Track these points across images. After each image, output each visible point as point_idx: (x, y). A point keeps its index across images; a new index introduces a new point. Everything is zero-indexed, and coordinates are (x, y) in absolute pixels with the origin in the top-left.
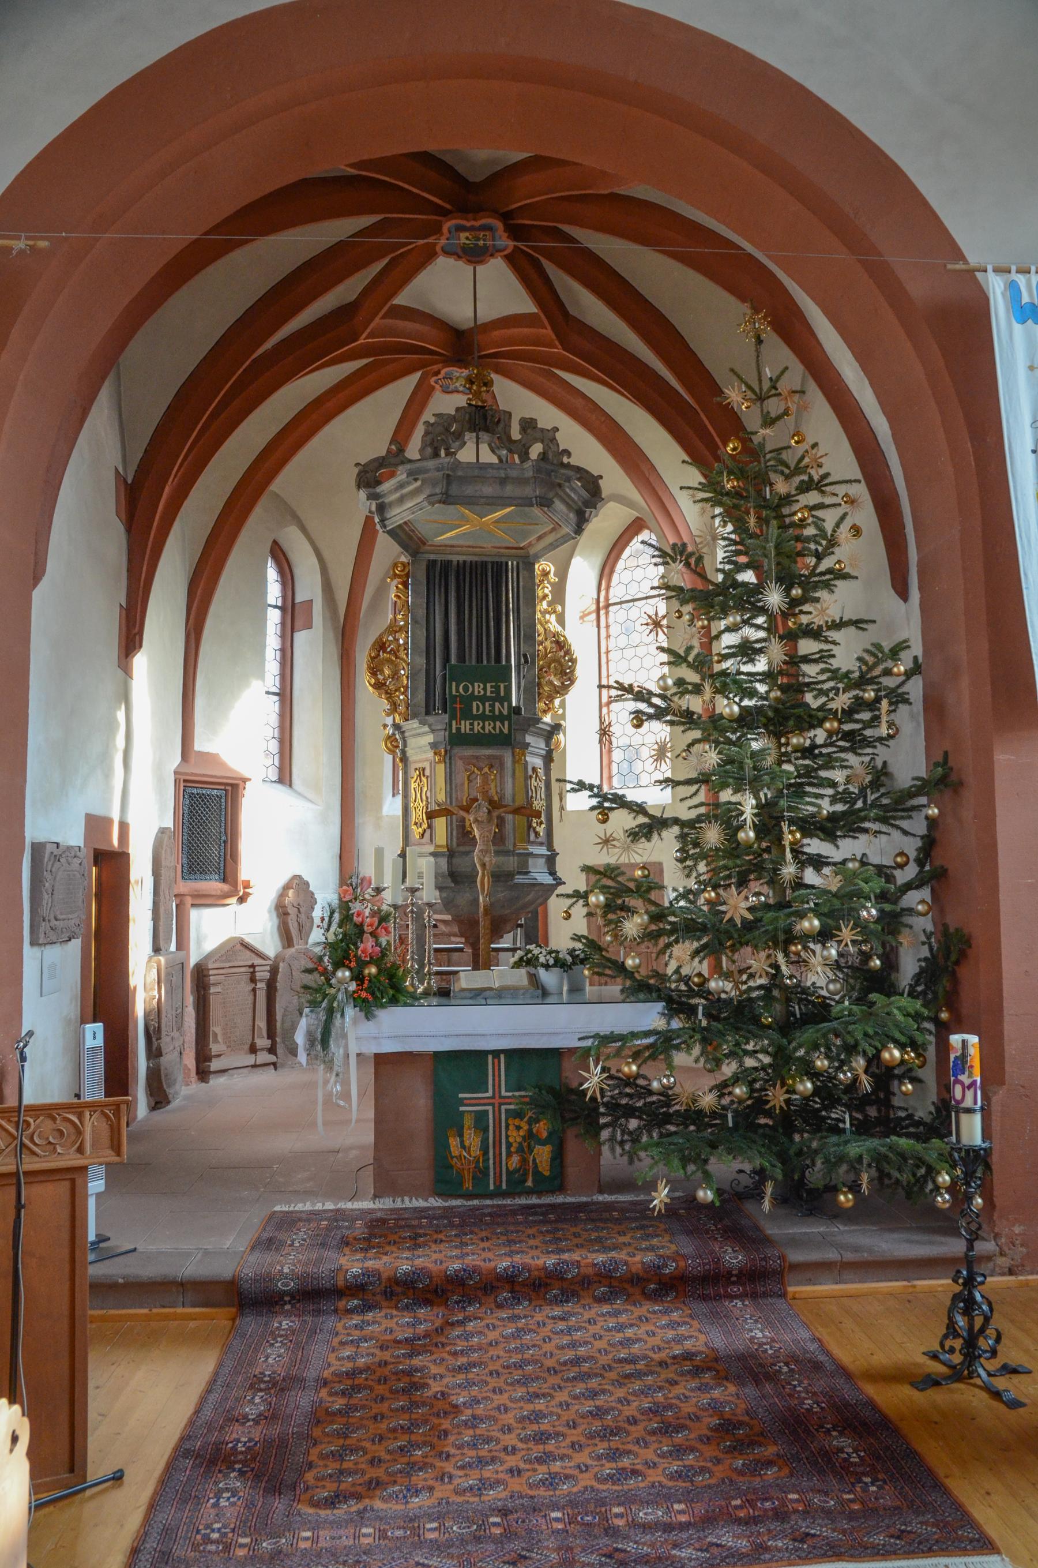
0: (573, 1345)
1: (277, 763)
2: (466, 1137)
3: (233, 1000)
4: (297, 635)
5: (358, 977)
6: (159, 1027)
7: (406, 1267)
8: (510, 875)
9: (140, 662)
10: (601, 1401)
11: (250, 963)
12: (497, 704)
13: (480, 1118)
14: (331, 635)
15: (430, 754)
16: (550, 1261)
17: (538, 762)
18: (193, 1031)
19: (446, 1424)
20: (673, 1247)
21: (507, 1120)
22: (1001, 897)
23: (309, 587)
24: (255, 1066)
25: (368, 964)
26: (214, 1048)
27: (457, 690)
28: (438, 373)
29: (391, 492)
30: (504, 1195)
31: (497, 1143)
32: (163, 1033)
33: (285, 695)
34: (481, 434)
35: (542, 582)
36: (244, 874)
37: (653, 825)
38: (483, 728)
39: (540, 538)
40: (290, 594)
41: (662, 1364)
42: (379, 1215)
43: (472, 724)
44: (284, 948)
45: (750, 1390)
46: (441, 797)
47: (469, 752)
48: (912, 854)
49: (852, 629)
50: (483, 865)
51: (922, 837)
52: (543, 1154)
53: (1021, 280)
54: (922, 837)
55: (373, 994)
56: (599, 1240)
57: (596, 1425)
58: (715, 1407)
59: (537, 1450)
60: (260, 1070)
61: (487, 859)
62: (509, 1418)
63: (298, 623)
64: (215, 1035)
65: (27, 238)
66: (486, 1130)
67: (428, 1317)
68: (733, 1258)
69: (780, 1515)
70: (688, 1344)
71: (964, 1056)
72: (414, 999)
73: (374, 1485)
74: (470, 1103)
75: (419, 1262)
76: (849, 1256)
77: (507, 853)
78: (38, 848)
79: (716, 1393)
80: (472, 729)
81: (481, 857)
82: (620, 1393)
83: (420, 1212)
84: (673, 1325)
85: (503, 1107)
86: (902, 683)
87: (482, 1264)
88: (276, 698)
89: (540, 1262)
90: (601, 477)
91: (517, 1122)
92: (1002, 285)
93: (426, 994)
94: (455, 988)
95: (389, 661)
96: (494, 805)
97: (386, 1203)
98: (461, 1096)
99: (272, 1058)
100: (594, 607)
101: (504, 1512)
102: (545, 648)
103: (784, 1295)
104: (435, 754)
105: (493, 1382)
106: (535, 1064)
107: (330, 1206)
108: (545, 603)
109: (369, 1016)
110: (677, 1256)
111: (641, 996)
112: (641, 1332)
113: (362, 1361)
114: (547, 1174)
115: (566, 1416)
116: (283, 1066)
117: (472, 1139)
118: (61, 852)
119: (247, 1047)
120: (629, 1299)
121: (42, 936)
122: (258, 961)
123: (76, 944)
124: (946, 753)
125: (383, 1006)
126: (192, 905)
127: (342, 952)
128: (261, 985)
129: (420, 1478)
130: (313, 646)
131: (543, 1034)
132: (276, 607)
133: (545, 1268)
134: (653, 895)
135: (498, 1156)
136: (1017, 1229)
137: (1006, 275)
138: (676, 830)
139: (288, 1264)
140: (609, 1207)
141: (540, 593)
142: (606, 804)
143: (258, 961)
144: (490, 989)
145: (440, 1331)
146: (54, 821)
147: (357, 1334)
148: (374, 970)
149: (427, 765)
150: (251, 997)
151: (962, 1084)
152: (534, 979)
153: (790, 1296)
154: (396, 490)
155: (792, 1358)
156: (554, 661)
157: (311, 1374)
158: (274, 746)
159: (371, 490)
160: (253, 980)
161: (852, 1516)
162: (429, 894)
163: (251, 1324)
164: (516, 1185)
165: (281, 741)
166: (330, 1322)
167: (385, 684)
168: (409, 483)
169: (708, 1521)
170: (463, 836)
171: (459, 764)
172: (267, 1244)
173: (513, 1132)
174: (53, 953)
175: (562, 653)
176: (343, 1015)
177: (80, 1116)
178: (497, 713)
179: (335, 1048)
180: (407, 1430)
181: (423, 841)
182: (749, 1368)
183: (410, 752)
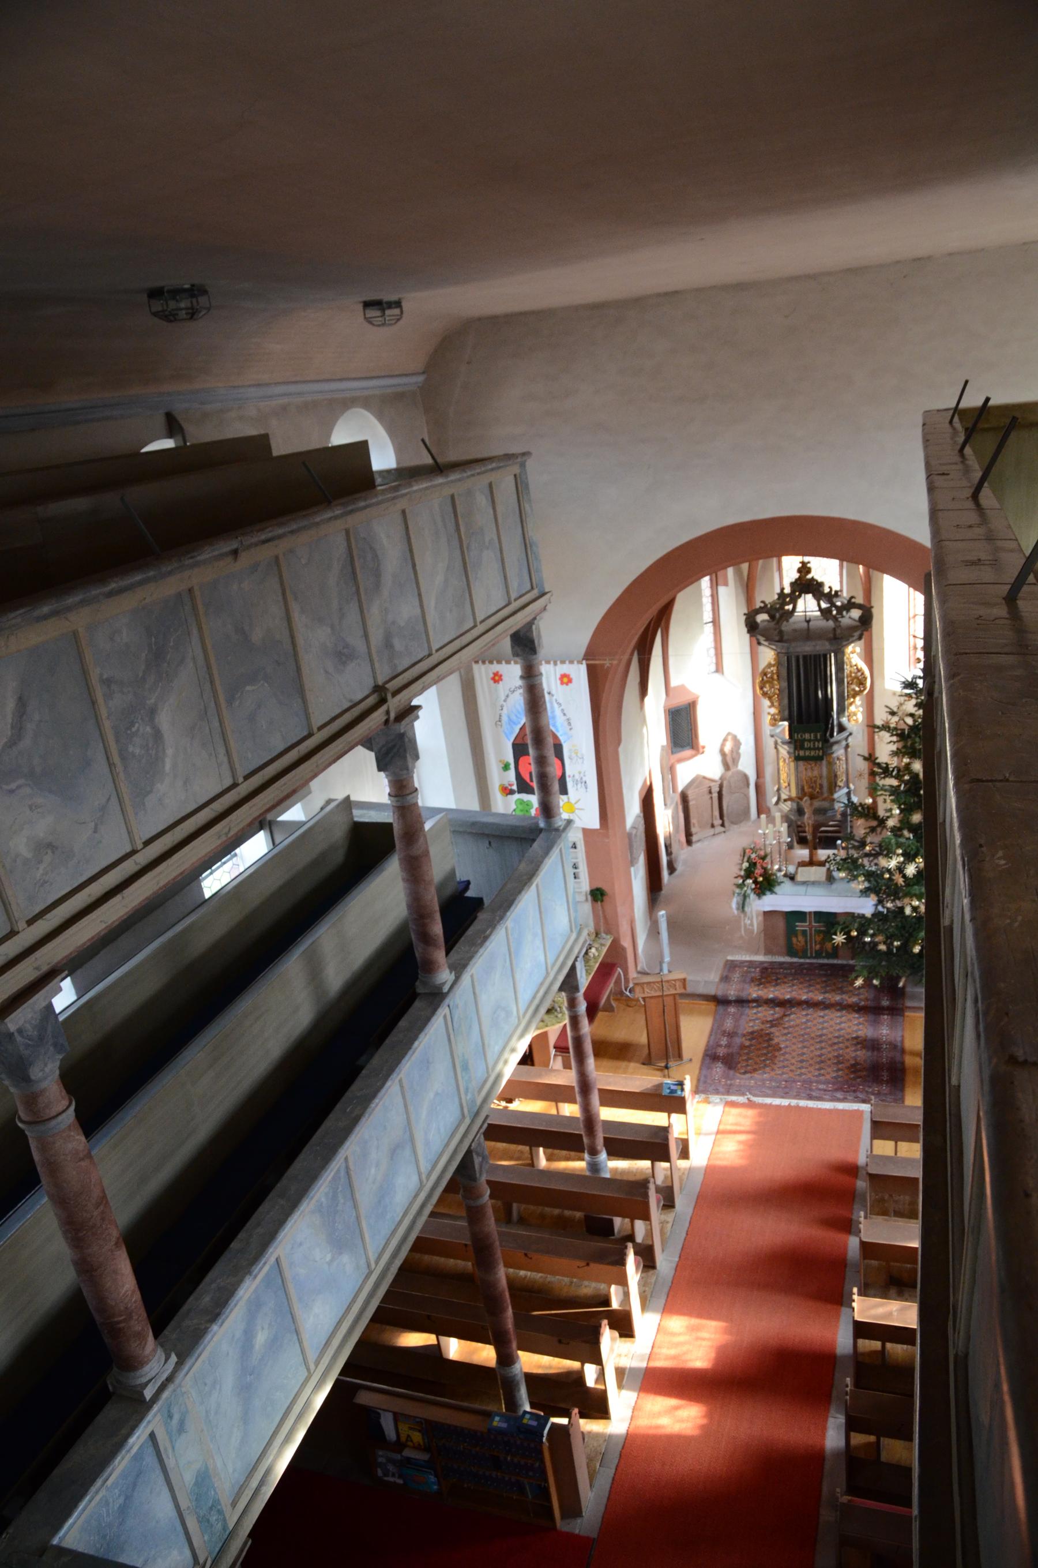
3: (701, 805)
5: (755, 882)
7: (771, 996)
10: (824, 1051)
13: (804, 932)
14: (740, 590)
16: (820, 998)
26: (693, 830)
30: (815, 958)
33: (716, 622)
41: (848, 1040)
45: (869, 1054)
56: (841, 989)
58: (855, 1058)
59: (800, 1065)
63: (720, 581)
69: (854, 1091)
73: (755, 1070)
74: (801, 926)
75: (777, 993)
83: (781, 964)
99: (722, 829)
105: (794, 1040)
107: (748, 958)
110: (867, 999)
117: (800, 938)
122: (712, 784)
129: (768, 1069)
135: (811, 947)
139: (732, 993)
145: (782, 1018)
147: (755, 1017)
155: (890, 1043)
157: (740, 1032)
158: (712, 652)
160: (710, 792)
163: (721, 1008)
164: (818, 955)
166: (747, 1011)
169: (836, 1090)
170: (800, 812)
172: (725, 979)
182: (873, 1045)
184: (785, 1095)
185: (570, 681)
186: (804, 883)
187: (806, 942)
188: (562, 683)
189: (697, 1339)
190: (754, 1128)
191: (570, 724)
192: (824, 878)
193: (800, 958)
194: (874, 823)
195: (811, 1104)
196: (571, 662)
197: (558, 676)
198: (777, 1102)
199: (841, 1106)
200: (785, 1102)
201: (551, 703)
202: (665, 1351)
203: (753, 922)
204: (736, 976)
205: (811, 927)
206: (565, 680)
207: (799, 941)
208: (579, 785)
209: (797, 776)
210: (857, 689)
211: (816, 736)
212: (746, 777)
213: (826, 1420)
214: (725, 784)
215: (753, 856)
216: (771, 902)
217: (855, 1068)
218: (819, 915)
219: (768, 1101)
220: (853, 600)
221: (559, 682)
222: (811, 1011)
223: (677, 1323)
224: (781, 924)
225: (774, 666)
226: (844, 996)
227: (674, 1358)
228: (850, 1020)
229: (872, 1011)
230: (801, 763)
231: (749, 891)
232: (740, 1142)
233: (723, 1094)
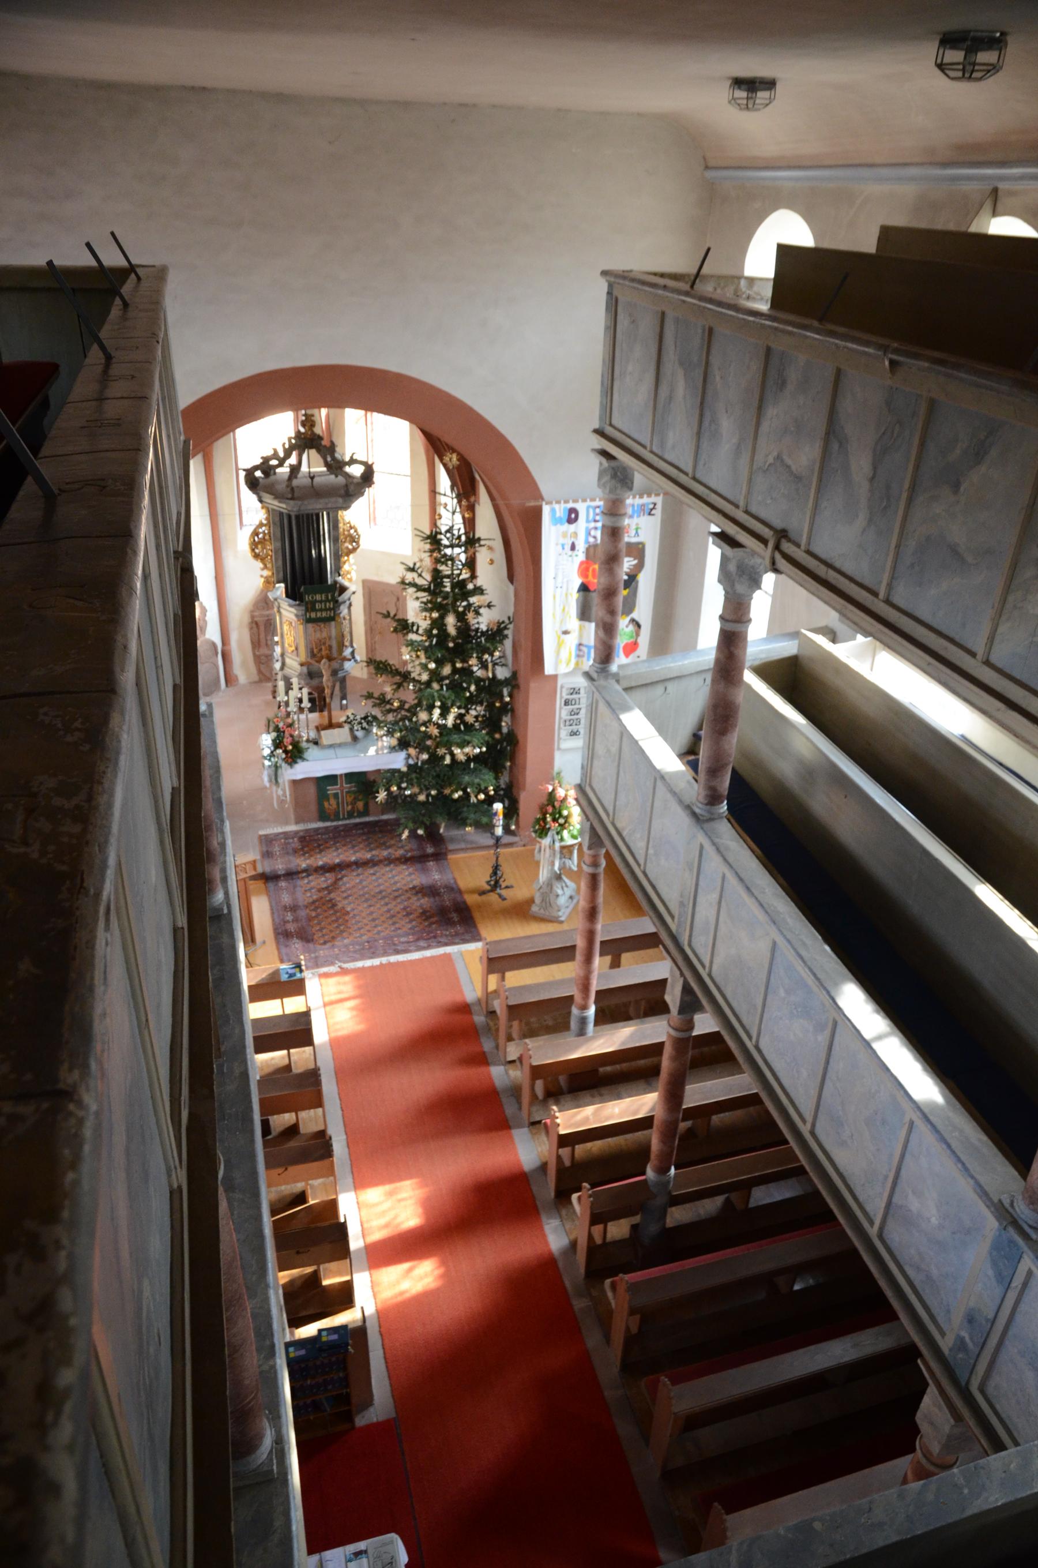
0: (379, 885)
5: (286, 752)
10: (389, 906)
13: (336, 796)
16: (369, 856)
41: (407, 891)
42: (302, 834)
45: (432, 900)
52: (360, 805)
53: (556, 506)
56: (384, 844)
58: (421, 906)
59: (373, 924)
67: (330, 877)
68: (430, 850)
69: (435, 937)
73: (333, 938)
74: (332, 790)
76: (469, 846)
79: (422, 901)
82: (394, 903)
83: (316, 830)
84: (410, 874)
110: (411, 850)
113: (315, 897)
117: (333, 802)
139: (280, 866)
155: (446, 887)
157: (301, 904)
161: (452, 936)
163: (271, 885)
164: (350, 815)
166: (299, 882)
169: (418, 940)
172: (267, 855)
179: (280, 780)
180: (336, 921)
182: (431, 891)
184: (374, 955)
186: (331, 746)
187: (338, 804)
189: (400, 1201)
192: (349, 739)
193: (332, 821)
194: (398, 679)
198: (368, 963)
199: (428, 953)
200: (376, 962)
202: (376, 1223)
203: (284, 792)
204: (276, 849)
205: (342, 788)
207: (331, 805)
209: (306, 639)
210: (350, 547)
212: (214, 645)
213: (542, 1229)
215: (281, 725)
216: (302, 770)
217: (425, 915)
218: (350, 777)
219: (359, 964)
222: (360, 870)
223: (374, 1194)
225: (265, 525)
226: (390, 850)
227: (386, 1226)
228: (400, 873)
229: (419, 859)
230: (310, 625)
231: (280, 762)
232: (352, 1009)
233: (313, 968)
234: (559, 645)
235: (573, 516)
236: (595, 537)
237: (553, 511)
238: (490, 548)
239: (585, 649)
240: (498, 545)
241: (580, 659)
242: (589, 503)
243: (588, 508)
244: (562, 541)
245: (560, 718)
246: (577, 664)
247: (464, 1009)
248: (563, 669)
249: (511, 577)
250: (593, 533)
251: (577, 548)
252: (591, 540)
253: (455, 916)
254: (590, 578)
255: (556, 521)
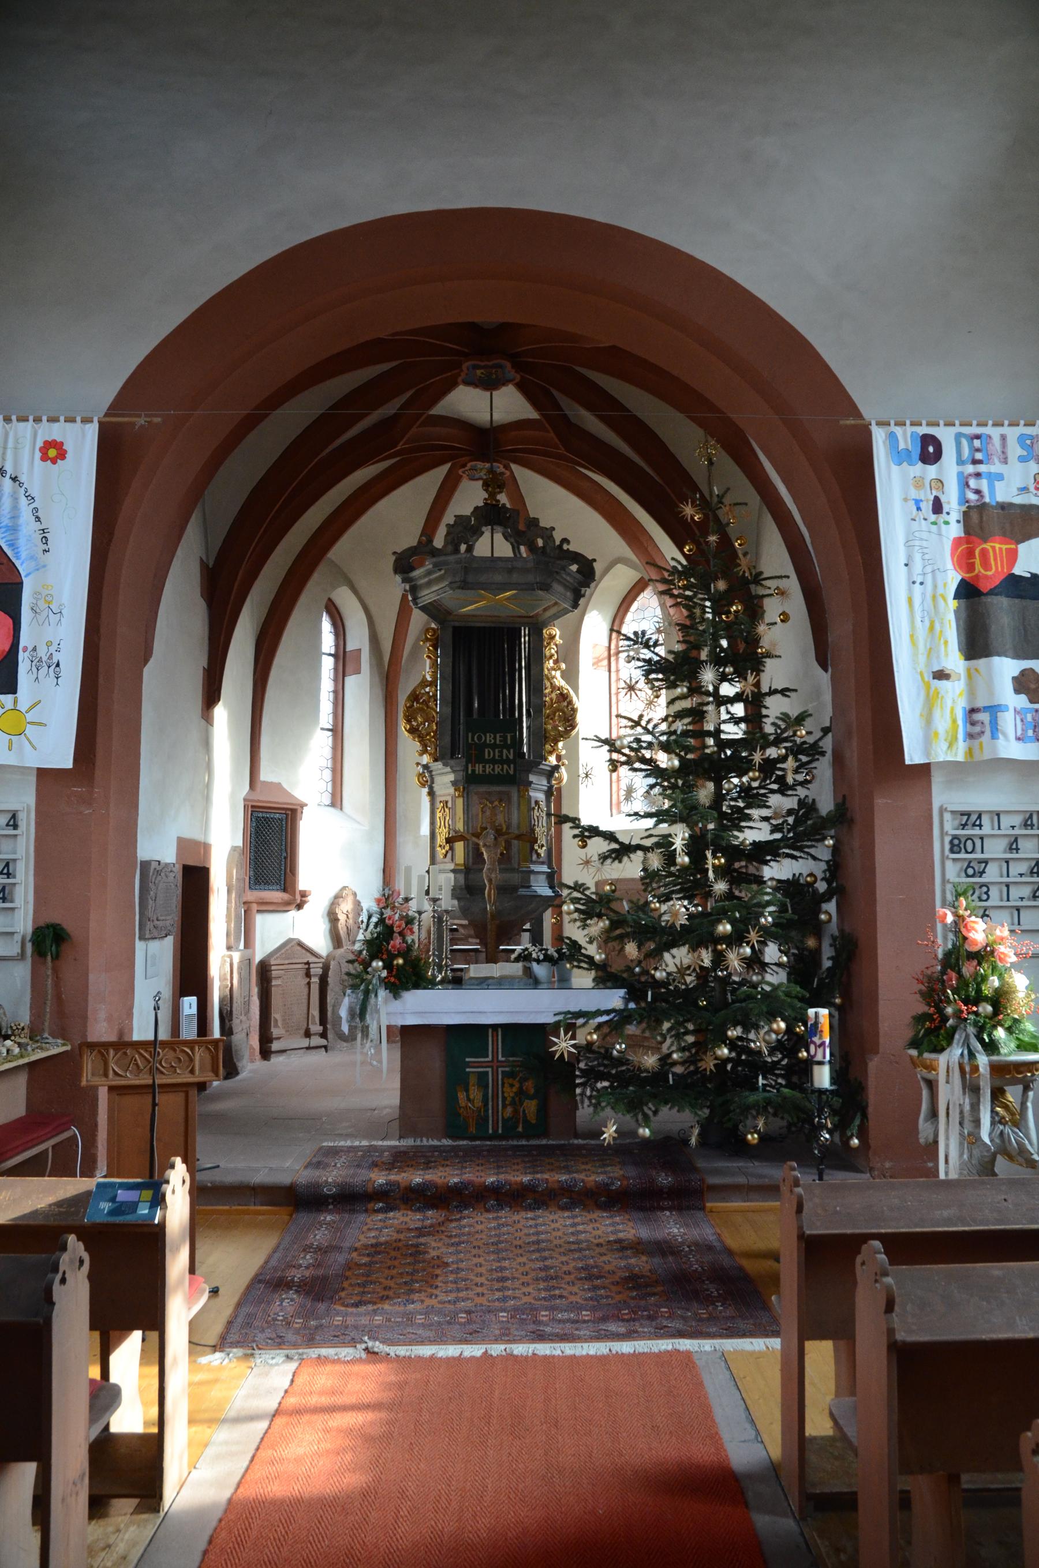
1: (330, 789)
2: (471, 1092)
3: (291, 993)
4: (347, 679)
6: (231, 1011)
7: (418, 1180)
8: (515, 889)
9: (220, 712)
11: (305, 961)
12: (505, 751)
14: (377, 679)
15: (452, 790)
17: (541, 796)
18: (258, 1017)
19: (438, 1272)
20: (621, 1172)
21: (502, 1079)
22: (878, 909)
23: (358, 639)
24: (308, 1048)
25: (396, 957)
26: (275, 1032)
27: (473, 739)
28: (464, 466)
29: (420, 578)
30: (501, 1138)
31: (495, 1096)
32: (234, 1016)
33: (337, 731)
34: (495, 527)
35: (549, 644)
36: (302, 885)
37: (623, 851)
38: (493, 770)
39: (545, 610)
40: (342, 643)
41: (599, 1245)
42: (402, 1149)
43: (484, 767)
44: (334, 948)
46: (460, 826)
47: (483, 789)
48: (820, 875)
49: (779, 696)
50: (490, 881)
51: (827, 862)
52: (531, 1106)
53: (898, 431)
54: (827, 862)
55: (400, 980)
56: (566, 1167)
57: (543, 1274)
58: (627, 1268)
60: (314, 1052)
61: (493, 876)
62: (483, 1270)
63: (348, 669)
64: (276, 1021)
65: (146, 416)
66: (487, 1086)
68: (664, 1179)
70: (621, 1235)
71: (816, 1023)
72: (431, 984)
73: (384, 1298)
75: (428, 1177)
76: (754, 1181)
77: (513, 870)
78: (145, 865)
79: (633, 1261)
80: (484, 771)
81: (489, 875)
83: (434, 1148)
85: (500, 1070)
86: (820, 739)
87: (475, 1179)
88: (330, 733)
89: (519, 1179)
90: (595, 560)
91: (511, 1081)
92: (883, 435)
93: (442, 982)
94: (466, 977)
95: (421, 710)
96: (499, 832)
97: (409, 1142)
98: (467, 1060)
99: (323, 1042)
100: (606, 654)
101: (469, 1312)
102: (551, 699)
103: (703, 1209)
104: (456, 790)
106: (527, 1039)
107: (365, 1143)
108: (551, 661)
109: (396, 996)
111: (609, 984)
112: (589, 1228)
113: (383, 1239)
114: (534, 1122)
115: (521, 1269)
116: (333, 1049)
117: (475, 1093)
118: (161, 868)
119: (302, 1032)
120: (586, 1208)
121: (148, 932)
122: (312, 959)
123: (170, 940)
124: (844, 796)
125: (407, 989)
126: (258, 911)
127: (377, 946)
128: (315, 980)
129: (416, 1296)
130: (360, 689)
131: (531, 1012)
132: (330, 655)
133: (522, 1183)
134: (614, 905)
136: (888, 1165)
137: (888, 428)
138: (640, 853)
139: (333, 1176)
140: (580, 1147)
141: (548, 653)
142: (586, 834)
143: (312, 959)
144: (493, 978)
146: (158, 846)
147: (380, 1225)
148: (401, 961)
149: (449, 799)
150: (306, 990)
151: (815, 1043)
152: (528, 972)
153: (707, 1209)
154: (425, 576)
156: (559, 710)
158: (328, 775)
159: (406, 575)
160: (308, 975)
162: (447, 902)
163: (304, 1218)
165: (334, 770)
166: (362, 1217)
167: (417, 730)
168: (434, 572)
169: (604, 1319)
170: (475, 856)
171: (475, 799)
173: (507, 1089)
174: (154, 946)
175: (565, 704)
176: (376, 995)
177: (192, 1050)
178: (504, 757)
181: (446, 860)
183: (436, 787)
185: (62, 455)
188: (45, 458)
190: (385, 1396)
191: (45, 540)
195: (544, 1349)
196: (71, 420)
197: (39, 444)
199: (626, 1347)
201: (15, 499)
206: (52, 453)
207: (470, 1099)
208: (44, 670)
211: (505, 739)
214: (332, 963)
217: (633, 1281)
219: (426, 1351)
220: (565, 547)
221: (38, 455)
224: (433, 1060)
233: (295, 1346)
234: (930, 703)
235: (931, 449)
236: (978, 492)
237: (892, 437)
238: (782, 593)
239: (984, 717)
240: (793, 585)
241: (976, 742)
242: (958, 429)
243: (958, 436)
244: (914, 494)
245: (944, 881)
246: (970, 752)
247: (718, 1485)
248: (941, 754)
249: (823, 662)
250: (973, 483)
251: (946, 508)
252: (972, 496)
253: (713, 1290)
254: (978, 567)
255: (900, 457)
